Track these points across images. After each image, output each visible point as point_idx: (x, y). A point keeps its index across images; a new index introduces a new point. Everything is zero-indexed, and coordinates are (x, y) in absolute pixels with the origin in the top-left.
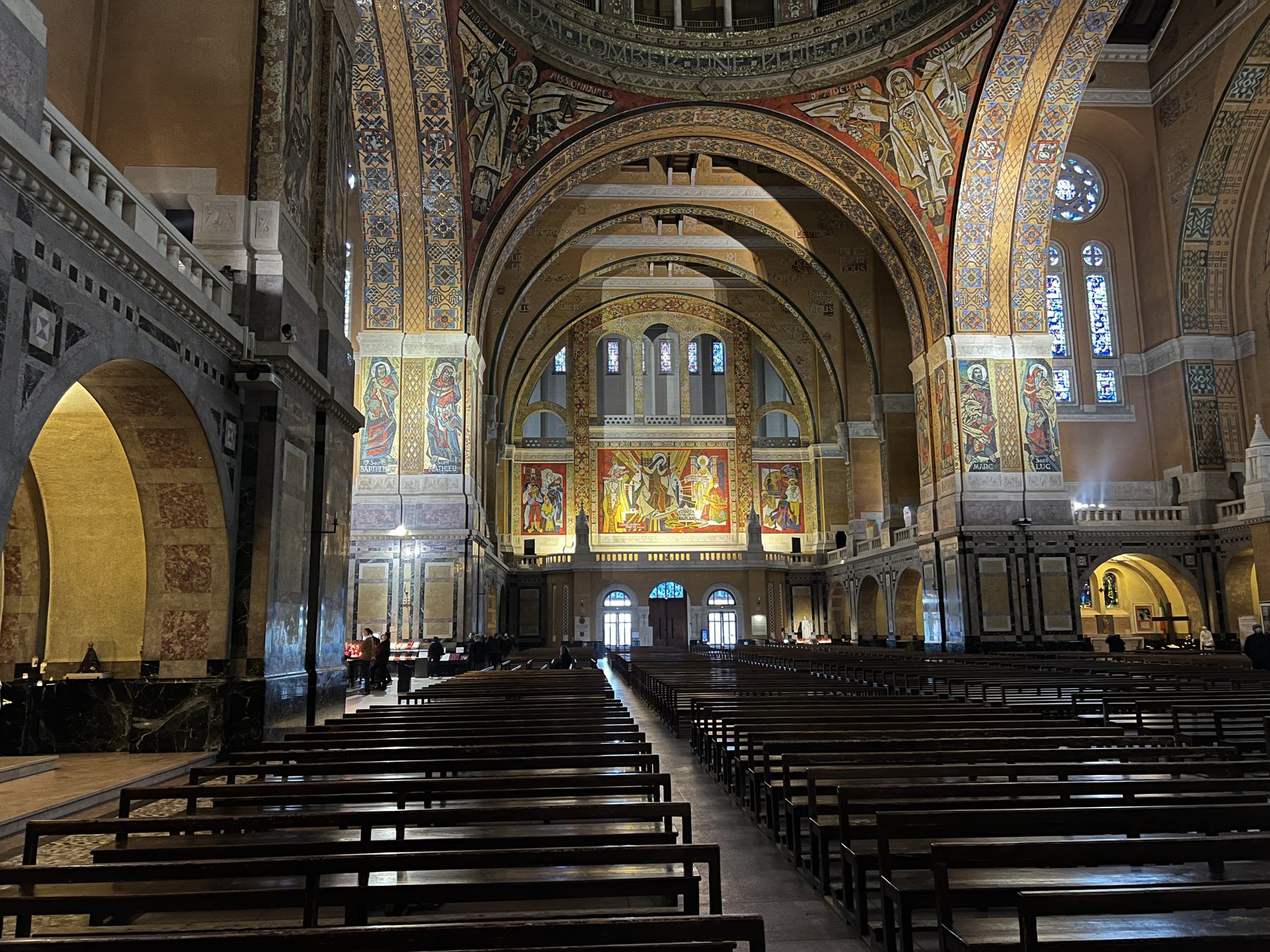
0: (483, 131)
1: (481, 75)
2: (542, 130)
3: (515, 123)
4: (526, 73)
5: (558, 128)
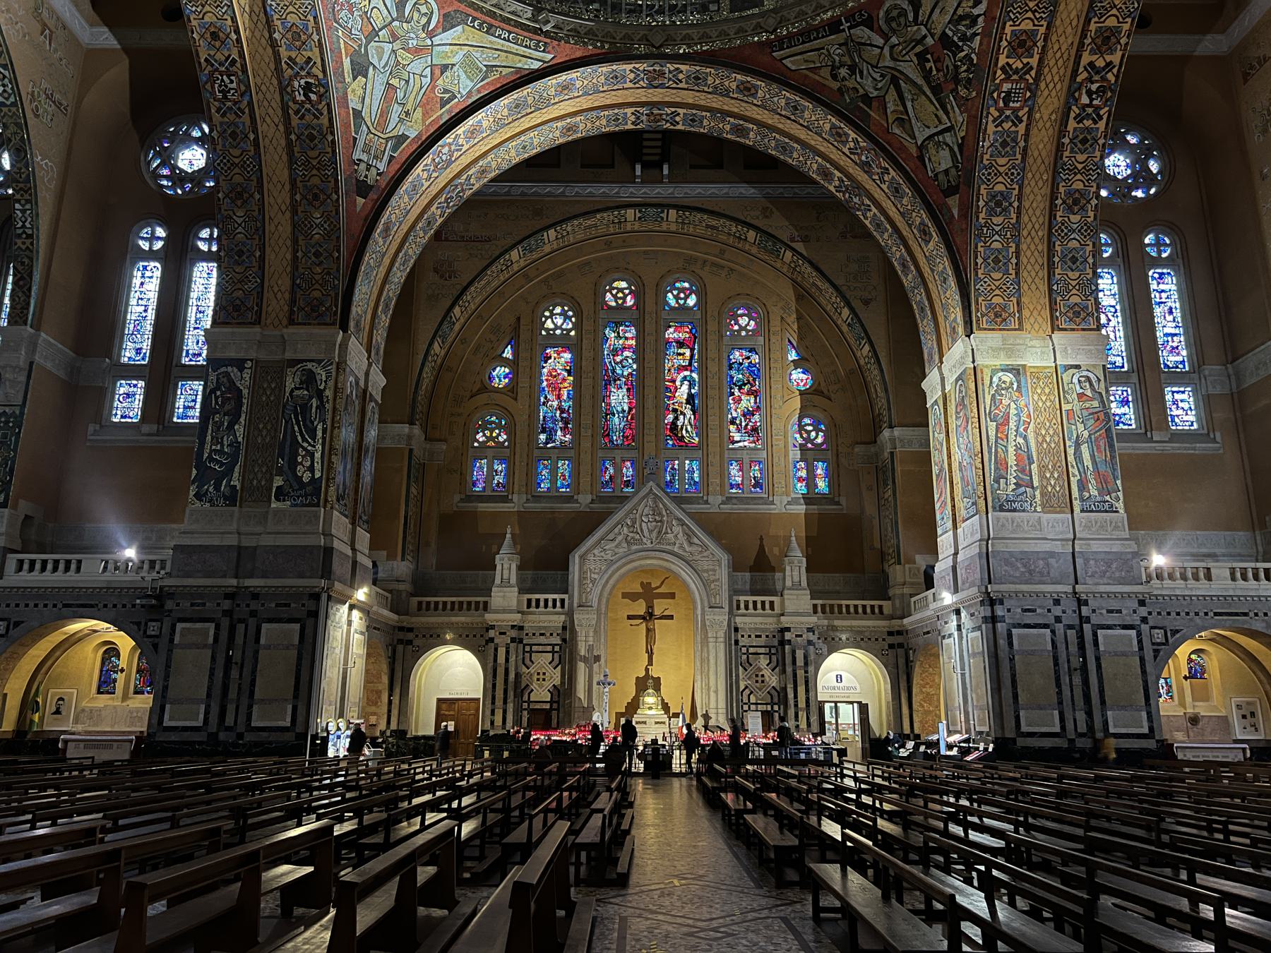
0: (901, 108)
1: (853, 69)
2: (964, 38)
3: (928, 65)
4: (895, 13)
5: (979, 16)
